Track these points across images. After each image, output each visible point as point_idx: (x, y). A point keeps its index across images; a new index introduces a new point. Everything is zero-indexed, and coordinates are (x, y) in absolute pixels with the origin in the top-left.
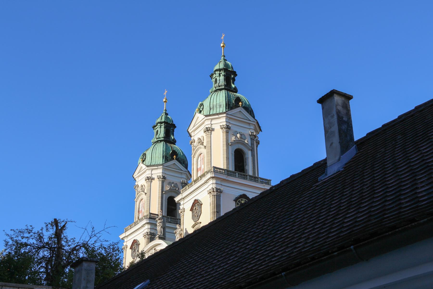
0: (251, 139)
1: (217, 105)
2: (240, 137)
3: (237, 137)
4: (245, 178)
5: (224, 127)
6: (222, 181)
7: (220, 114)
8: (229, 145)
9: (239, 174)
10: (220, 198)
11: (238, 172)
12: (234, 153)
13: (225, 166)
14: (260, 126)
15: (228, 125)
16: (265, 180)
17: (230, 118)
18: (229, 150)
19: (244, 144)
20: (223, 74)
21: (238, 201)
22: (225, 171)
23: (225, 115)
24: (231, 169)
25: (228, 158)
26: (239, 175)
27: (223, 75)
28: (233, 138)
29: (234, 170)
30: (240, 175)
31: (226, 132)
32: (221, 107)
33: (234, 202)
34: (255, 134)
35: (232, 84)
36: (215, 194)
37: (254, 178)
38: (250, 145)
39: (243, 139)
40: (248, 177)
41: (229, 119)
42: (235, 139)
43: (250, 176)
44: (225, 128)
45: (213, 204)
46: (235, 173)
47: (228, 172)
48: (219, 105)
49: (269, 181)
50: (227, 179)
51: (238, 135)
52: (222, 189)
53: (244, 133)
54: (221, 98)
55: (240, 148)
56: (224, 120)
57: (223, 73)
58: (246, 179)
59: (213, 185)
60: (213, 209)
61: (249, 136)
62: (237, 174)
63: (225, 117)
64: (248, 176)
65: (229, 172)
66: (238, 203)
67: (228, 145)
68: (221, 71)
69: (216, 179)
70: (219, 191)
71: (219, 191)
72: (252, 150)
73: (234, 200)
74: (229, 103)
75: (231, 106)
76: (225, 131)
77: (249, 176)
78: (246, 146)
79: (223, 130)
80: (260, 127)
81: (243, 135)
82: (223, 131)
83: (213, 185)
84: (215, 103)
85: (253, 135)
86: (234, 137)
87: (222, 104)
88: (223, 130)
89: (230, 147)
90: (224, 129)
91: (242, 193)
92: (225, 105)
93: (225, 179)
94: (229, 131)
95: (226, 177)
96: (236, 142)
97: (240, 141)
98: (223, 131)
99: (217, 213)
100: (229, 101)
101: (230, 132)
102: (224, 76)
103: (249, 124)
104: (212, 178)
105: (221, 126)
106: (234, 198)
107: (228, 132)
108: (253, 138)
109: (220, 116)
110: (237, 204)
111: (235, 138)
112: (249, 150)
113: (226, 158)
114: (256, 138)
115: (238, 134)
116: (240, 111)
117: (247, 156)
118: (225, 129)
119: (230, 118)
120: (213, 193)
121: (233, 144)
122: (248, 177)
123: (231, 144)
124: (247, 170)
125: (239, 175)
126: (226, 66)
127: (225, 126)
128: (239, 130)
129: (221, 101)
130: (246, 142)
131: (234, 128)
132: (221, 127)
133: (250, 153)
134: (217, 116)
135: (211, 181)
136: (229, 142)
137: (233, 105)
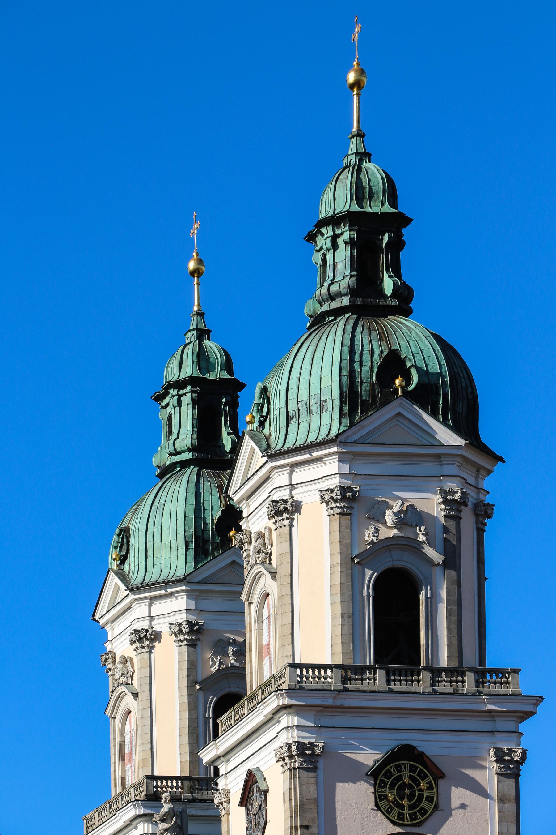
6: (321, 711)
19: (411, 546)
21: (385, 775)
32: (325, 408)
39: (411, 525)
41: (352, 459)
44: (336, 501)
45: (291, 800)
48: (319, 403)
60: (291, 817)
75: (364, 398)
76: (337, 511)
79: (332, 508)
82: (331, 512)
87: (326, 396)
88: (332, 508)
90: (333, 505)
92: (337, 402)
98: (331, 512)
99: (305, 831)
103: (439, 456)
113: (342, 617)
116: (399, 414)
129: (326, 382)
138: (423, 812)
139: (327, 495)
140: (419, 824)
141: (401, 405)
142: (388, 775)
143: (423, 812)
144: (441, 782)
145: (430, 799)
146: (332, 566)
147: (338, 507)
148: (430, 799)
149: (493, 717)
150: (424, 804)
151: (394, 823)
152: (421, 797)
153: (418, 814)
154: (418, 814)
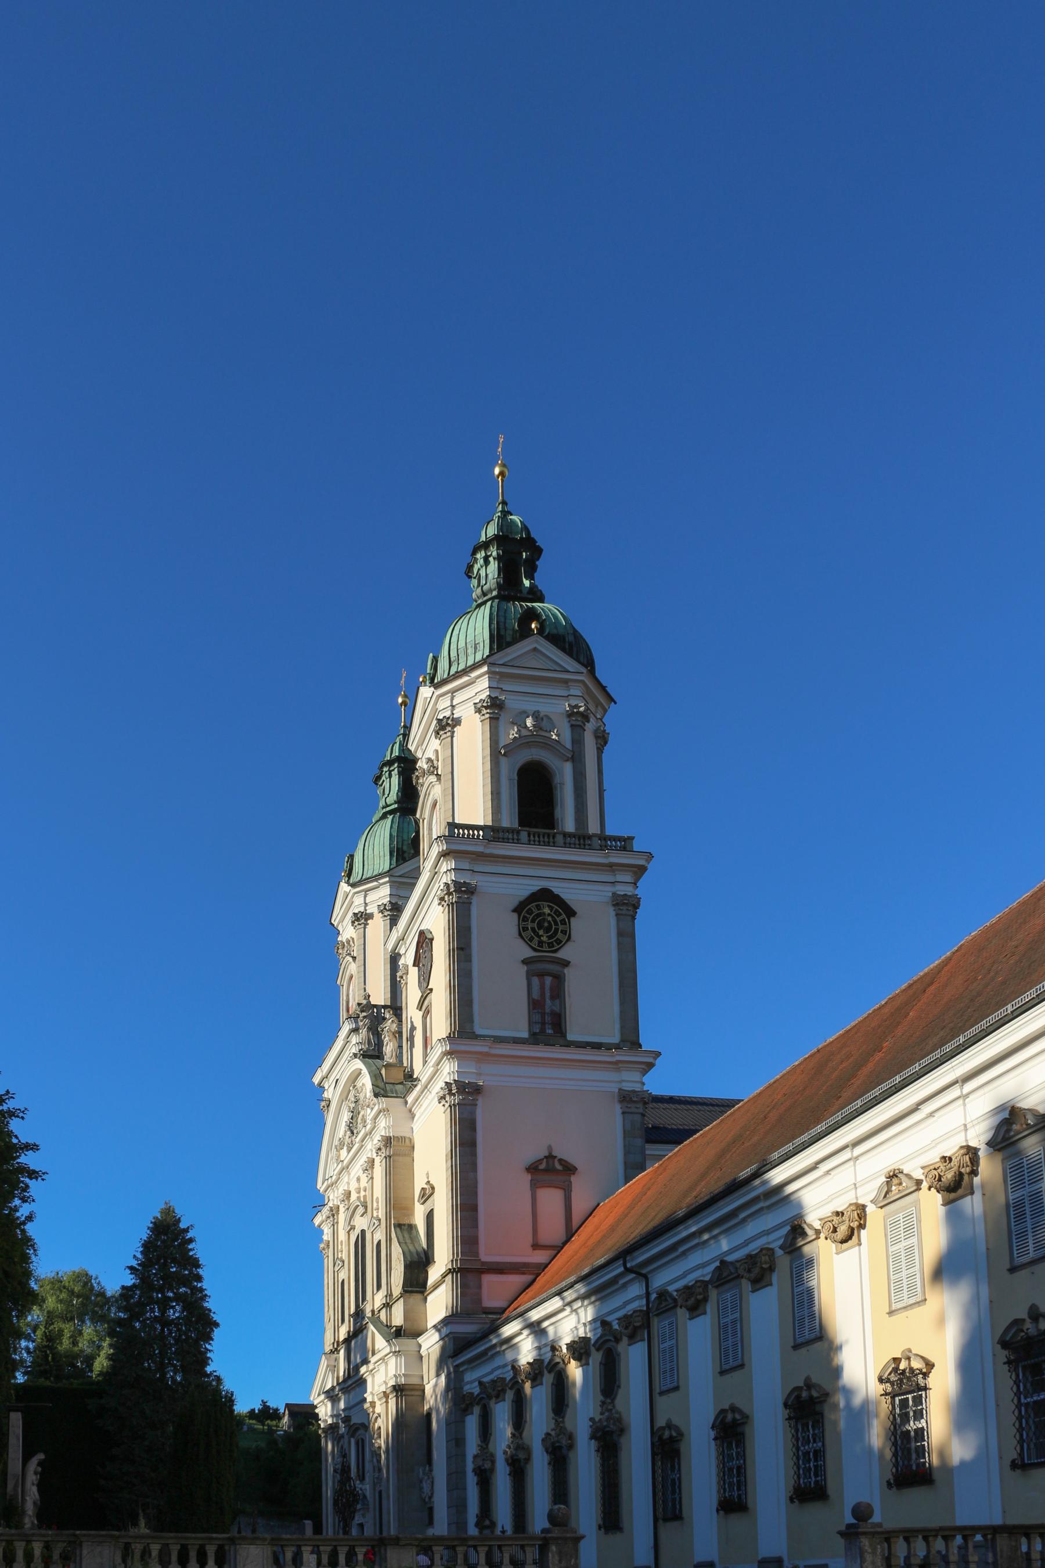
0: (572, 726)
1: (469, 646)
2: (534, 726)
3: (526, 727)
4: (549, 842)
5: (485, 704)
7: (473, 668)
8: (501, 757)
9: (529, 836)
10: (469, 910)
11: (528, 829)
12: (516, 778)
13: (490, 818)
14: (604, 685)
15: (497, 697)
16: (614, 840)
17: (502, 675)
18: (500, 771)
20: (495, 554)
21: (527, 912)
22: (485, 830)
23: (485, 669)
24: (506, 823)
25: (496, 794)
26: (532, 836)
27: (494, 558)
28: (513, 733)
29: (516, 825)
30: (534, 837)
31: (490, 718)
33: (515, 916)
34: (582, 709)
35: (524, 580)
36: (454, 900)
37: (579, 840)
38: (569, 745)
39: (546, 731)
40: (560, 839)
42: (517, 736)
43: (566, 835)
44: (486, 708)
45: (449, 929)
46: (518, 832)
47: (494, 833)
49: (627, 841)
50: (488, 851)
51: (529, 722)
52: (473, 882)
53: (547, 714)
54: (479, 625)
55: (536, 757)
56: (484, 683)
57: (494, 551)
58: (551, 844)
59: (447, 876)
60: (449, 943)
61: (566, 720)
62: (524, 835)
63: (487, 676)
64: (557, 835)
65: (498, 831)
66: (524, 917)
67: (497, 753)
68: (489, 546)
69: (454, 858)
70: (463, 889)
71: (463, 889)
72: (576, 757)
73: (514, 911)
74: (502, 633)
76: (487, 716)
77: (562, 836)
78: (555, 748)
79: (483, 715)
80: (603, 688)
81: (545, 719)
82: (483, 718)
83: (447, 876)
84: (462, 644)
85: (578, 712)
86: (516, 730)
87: (479, 640)
88: (483, 715)
89: (503, 761)
90: (484, 711)
91: (536, 886)
92: (487, 642)
93: (482, 852)
94: (500, 713)
95: (485, 846)
96: (523, 742)
97: (537, 738)
98: (483, 718)
99: (461, 952)
100: (502, 627)
101: (505, 718)
102: (499, 558)
103: (566, 682)
104: (444, 855)
105: (475, 704)
106: (515, 903)
107: (498, 718)
108: (578, 720)
109: (474, 674)
110: (523, 920)
111: (519, 730)
112: (567, 760)
113: (492, 794)
114: (588, 721)
115: (528, 717)
116: (535, 649)
117: (557, 780)
118: (488, 711)
119: (502, 675)
120: (449, 897)
121: (512, 748)
122: (560, 839)
123: (506, 750)
124: (558, 819)
125: (532, 836)
126: (505, 530)
127: (487, 702)
128: (531, 707)
129: (479, 631)
130: (554, 737)
131: (514, 703)
132: (475, 707)
133: (568, 768)
134: (465, 679)
135: (446, 865)
136: (502, 744)
137: (513, 635)
138: (559, 941)
139: (479, 706)
140: (556, 951)
141: (537, 642)
142: (530, 912)
143: (559, 941)
144: (572, 920)
145: (564, 932)
146: (484, 758)
147: (487, 713)
148: (564, 932)
149: (613, 871)
150: (559, 935)
151: (535, 950)
152: (556, 930)
153: (554, 943)
154: (554, 943)
